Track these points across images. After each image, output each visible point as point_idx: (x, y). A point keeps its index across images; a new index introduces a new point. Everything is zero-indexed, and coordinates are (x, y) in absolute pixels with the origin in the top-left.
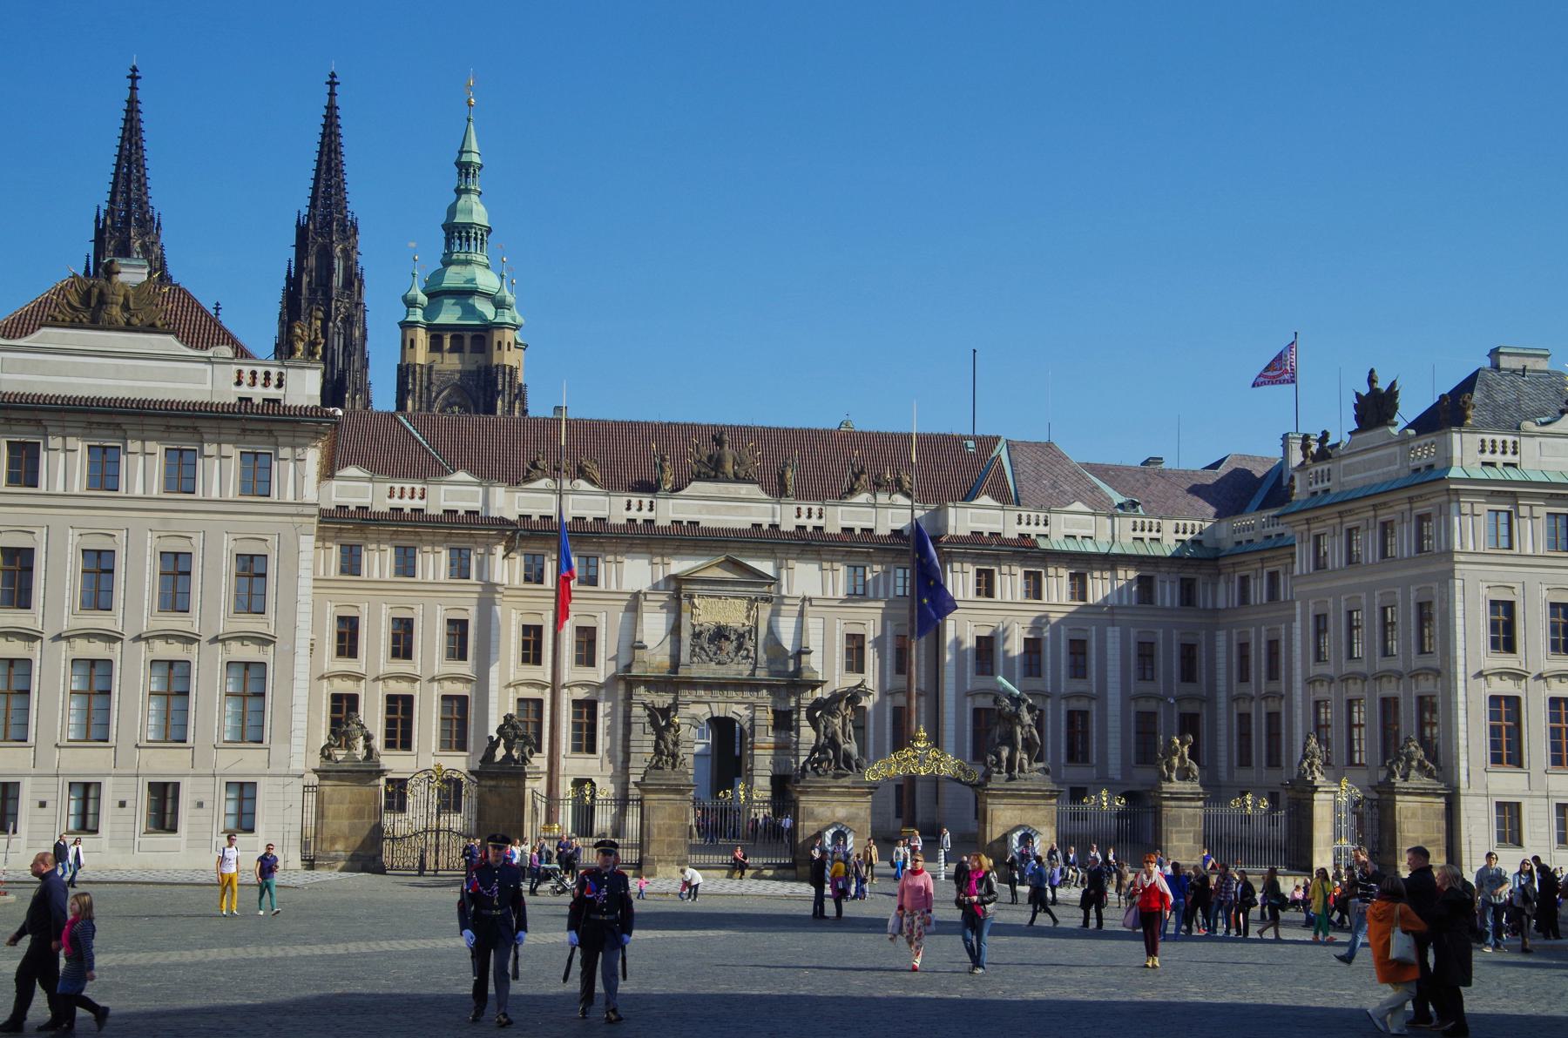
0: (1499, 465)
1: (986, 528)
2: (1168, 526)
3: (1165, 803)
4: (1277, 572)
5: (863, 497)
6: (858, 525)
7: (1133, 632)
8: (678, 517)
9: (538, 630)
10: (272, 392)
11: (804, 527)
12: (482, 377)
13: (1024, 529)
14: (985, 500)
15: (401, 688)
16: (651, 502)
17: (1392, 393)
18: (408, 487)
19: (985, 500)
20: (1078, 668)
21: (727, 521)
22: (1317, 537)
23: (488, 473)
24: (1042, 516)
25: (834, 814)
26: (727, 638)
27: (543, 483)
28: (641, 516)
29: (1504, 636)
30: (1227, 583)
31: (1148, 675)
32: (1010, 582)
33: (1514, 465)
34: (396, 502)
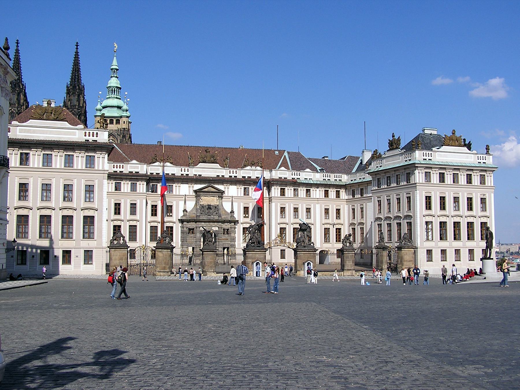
0: (427, 160)
1: (283, 176)
2: (332, 175)
3: (344, 252)
4: (363, 189)
5: (249, 168)
6: (247, 176)
7: (323, 206)
9: (156, 206)
10: (95, 138)
11: (232, 176)
12: (119, 132)
13: (293, 177)
14: (283, 168)
15: (117, 223)
16: (188, 169)
17: (399, 140)
18: (118, 165)
21: (208, 174)
23: (142, 160)
26: (210, 208)
27: (157, 164)
29: (429, 206)
30: (348, 192)
31: (327, 217)
34: (115, 169)
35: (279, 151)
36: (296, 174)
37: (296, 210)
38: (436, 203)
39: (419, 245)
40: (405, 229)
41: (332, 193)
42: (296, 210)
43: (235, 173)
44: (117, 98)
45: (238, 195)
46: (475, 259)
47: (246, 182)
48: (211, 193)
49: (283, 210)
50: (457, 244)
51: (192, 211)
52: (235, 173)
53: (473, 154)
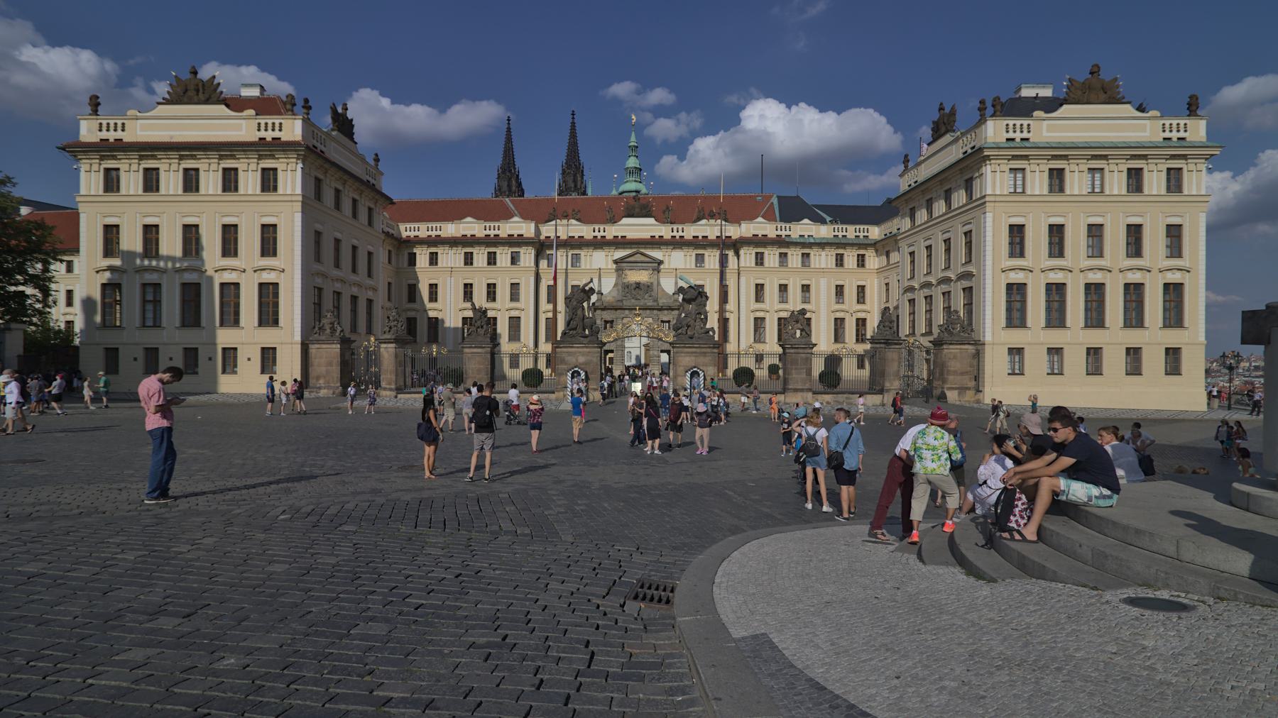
1: (760, 233)
2: (851, 228)
5: (704, 222)
6: (700, 235)
8: (616, 235)
13: (779, 233)
14: (760, 219)
17: (953, 113)
18: (492, 225)
19: (760, 219)
20: (806, 300)
23: (526, 216)
25: (577, 360)
27: (554, 222)
28: (599, 235)
32: (771, 256)
33: (1027, 139)
34: (488, 232)
35: (764, 197)
36: (783, 228)
37: (783, 288)
38: (1037, 240)
39: (988, 338)
42: (783, 288)
43: (680, 232)
44: (635, 181)
47: (698, 243)
48: (640, 264)
49: (759, 288)
51: (609, 293)
52: (680, 232)
53: (1149, 118)
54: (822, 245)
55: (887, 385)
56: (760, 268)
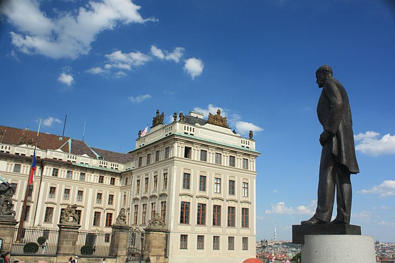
1: (58, 158)
2: (109, 163)
5: (24, 145)
6: (20, 153)
7: (97, 190)
13: (69, 159)
17: (163, 115)
19: (59, 150)
22: (141, 158)
24: (75, 156)
29: (187, 184)
31: (100, 202)
33: (193, 135)
35: (63, 137)
37: (67, 191)
38: (195, 182)
40: (159, 209)
41: (107, 179)
42: (67, 191)
45: (7, 170)
46: (249, 249)
47: (19, 159)
49: (53, 190)
50: (216, 230)
53: (237, 136)
54: (93, 170)
55: (119, 253)
56: (55, 178)
